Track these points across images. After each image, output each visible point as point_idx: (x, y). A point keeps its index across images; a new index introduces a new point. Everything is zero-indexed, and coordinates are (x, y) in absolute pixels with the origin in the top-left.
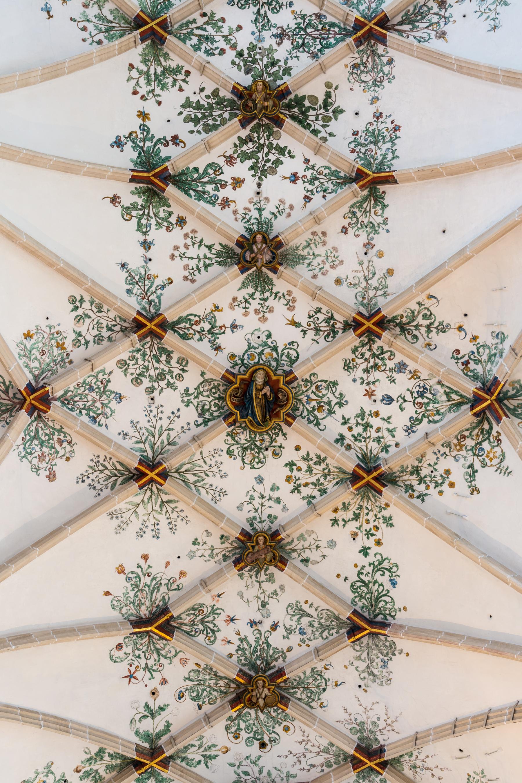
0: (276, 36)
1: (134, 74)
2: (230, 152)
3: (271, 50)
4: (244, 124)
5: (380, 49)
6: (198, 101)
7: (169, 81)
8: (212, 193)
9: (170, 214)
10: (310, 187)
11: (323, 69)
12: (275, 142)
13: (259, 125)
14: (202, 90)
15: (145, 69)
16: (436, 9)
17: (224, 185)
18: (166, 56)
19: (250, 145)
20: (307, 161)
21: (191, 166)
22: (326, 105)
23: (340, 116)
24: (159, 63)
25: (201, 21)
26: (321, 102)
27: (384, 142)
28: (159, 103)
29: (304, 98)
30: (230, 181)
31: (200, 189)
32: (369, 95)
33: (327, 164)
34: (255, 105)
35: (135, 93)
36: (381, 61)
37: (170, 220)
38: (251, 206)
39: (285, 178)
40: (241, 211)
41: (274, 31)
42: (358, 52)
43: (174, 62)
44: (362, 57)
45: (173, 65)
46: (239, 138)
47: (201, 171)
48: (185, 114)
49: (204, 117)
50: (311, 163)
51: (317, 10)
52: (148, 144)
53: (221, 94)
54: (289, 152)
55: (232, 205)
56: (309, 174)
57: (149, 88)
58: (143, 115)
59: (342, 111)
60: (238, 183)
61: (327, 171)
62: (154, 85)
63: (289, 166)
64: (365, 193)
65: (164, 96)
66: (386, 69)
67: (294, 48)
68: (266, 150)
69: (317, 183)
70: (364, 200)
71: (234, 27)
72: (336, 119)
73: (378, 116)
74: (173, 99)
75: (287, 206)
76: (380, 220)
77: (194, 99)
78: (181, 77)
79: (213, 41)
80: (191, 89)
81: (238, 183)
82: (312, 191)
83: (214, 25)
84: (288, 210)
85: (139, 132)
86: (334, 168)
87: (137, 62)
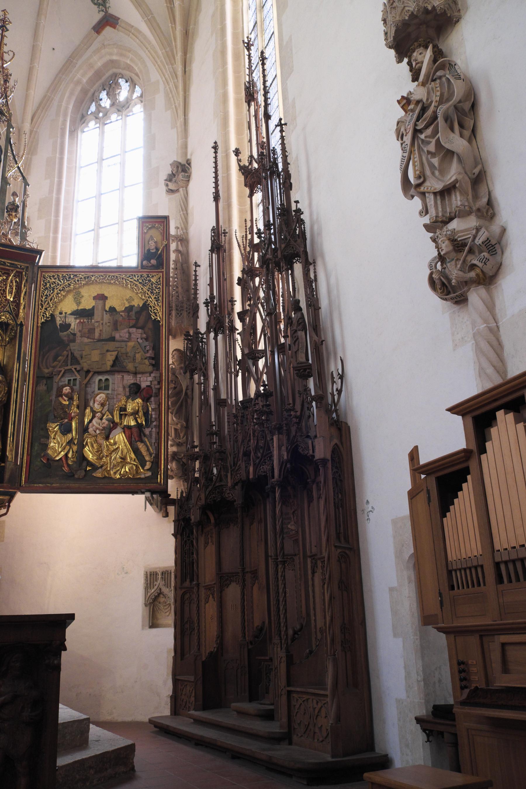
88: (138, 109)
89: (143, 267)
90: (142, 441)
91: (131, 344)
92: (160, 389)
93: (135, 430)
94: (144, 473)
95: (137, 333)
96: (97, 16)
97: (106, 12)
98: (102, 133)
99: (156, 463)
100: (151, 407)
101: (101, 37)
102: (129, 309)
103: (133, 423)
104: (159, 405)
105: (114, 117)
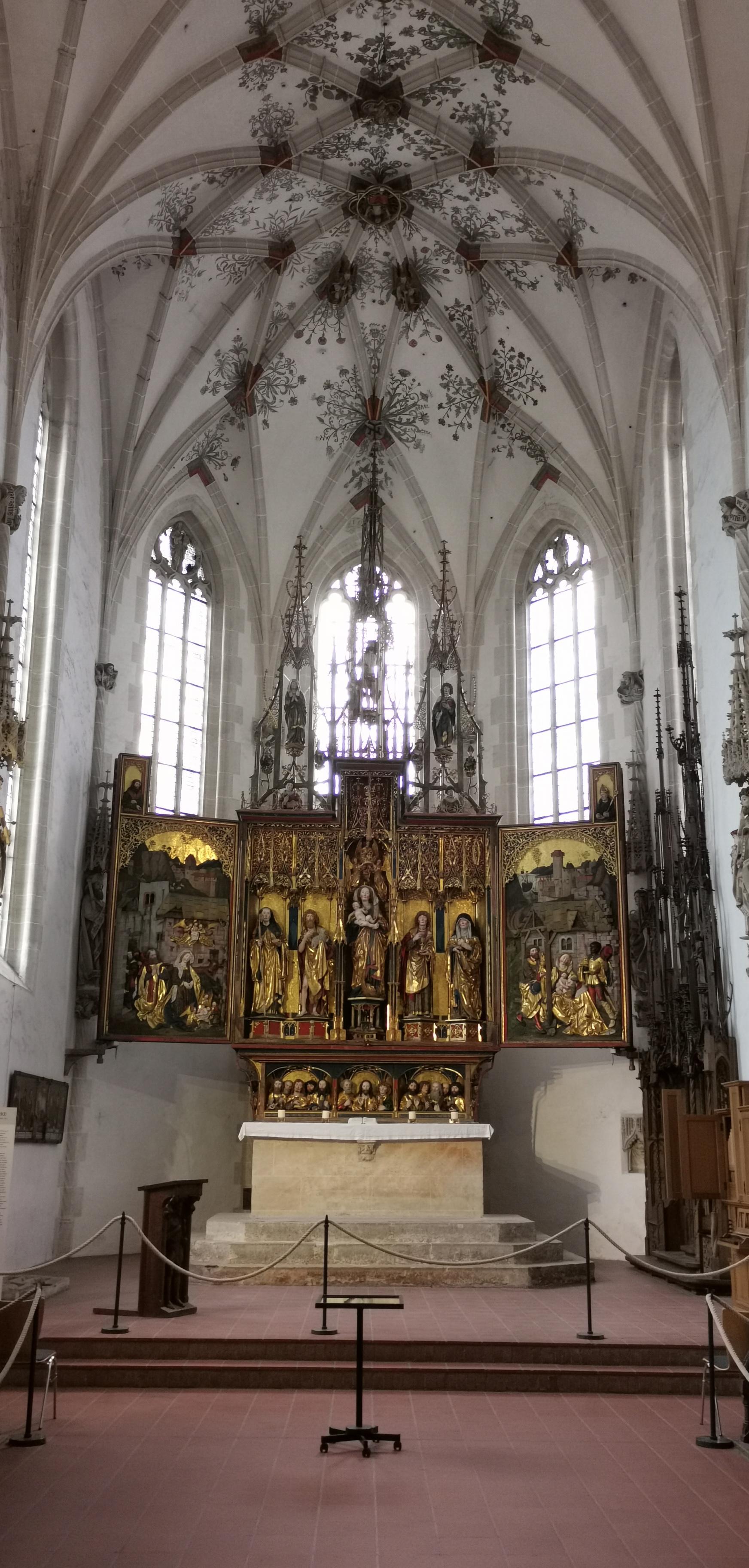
0: (366, 144)
1: (504, 126)
2: (414, 58)
3: (371, 134)
4: (398, 82)
5: (265, 142)
6: (444, 93)
7: (471, 111)
8: (435, 24)
9: (482, 9)
10: (329, 29)
11: (320, 127)
12: (367, 65)
13: (384, 79)
14: (440, 103)
15: (493, 126)
16: (217, 176)
17: (422, 30)
18: (472, 131)
19: (392, 63)
20: (334, 51)
21: (455, 50)
22: (315, 90)
23: (301, 82)
24: (480, 127)
25: (437, 154)
26: (321, 93)
27: (254, 70)
28: (483, 95)
29: (338, 98)
30: (415, 33)
31: (448, 29)
32: (273, 100)
33: (313, 50)
34: (387, 108)
35: (506, 111)
36: (263, 130)
37: (482, 4)
38: (394, 11)
39: (357, 36)
40: (405, 7)
41: (367, 147)
42: (285, 136)
43: (464, 128)
44: (282, 131)
45: (466, 124)
46: (404, 68)
47: (445, 45)
48: (458, 85)
49: (439, 83)
50: (329, 49)
51: (327, 162)
52: (499, 67)
53: (421, 102)
54: (352, 58)
55: (414, 12)
56: (331, 40)
57: (492, 110)
58: (500, 90)
59: (299, 86)
60: (407, 32)
61: (312, 43)
62: (486, 111)
63: (353, 47)
64: (271, 28)
65: (478, 100)
66: (258, 125)
67: (348, 136)
68: (377, 60)
69: (323, 33)
70: (271, 21)
71: (405, 149)
72: (304, 80)
73: (262, 87)
74: (470, 96)
75: (354, 13)
76: (253, 8)
77: (448, 96)
78: (460, 113)
79: (426, 141)
80: (450, 103)
81: (407, 32)
82: (328, 25)
83: (424, 151)
84: (353, 8)
85: (506, 79)
86: (305, 46)
87: (500, 135)
88: (588, 575)
89: (596, 820)
90: (605, 1000)
91: (589, 902)
92: (619, 948)
93: (598, 989)
94: (608, 1031)
95: (594, 891)
96: (535, 468)
97: (545, 462)
98: (551, 603)
99: (619, 1020)
100: (612, 965)
101: (541, 494)
102: (586, 864)
103: (597, 983)
104: (619, 963)
105: (563, 584)
